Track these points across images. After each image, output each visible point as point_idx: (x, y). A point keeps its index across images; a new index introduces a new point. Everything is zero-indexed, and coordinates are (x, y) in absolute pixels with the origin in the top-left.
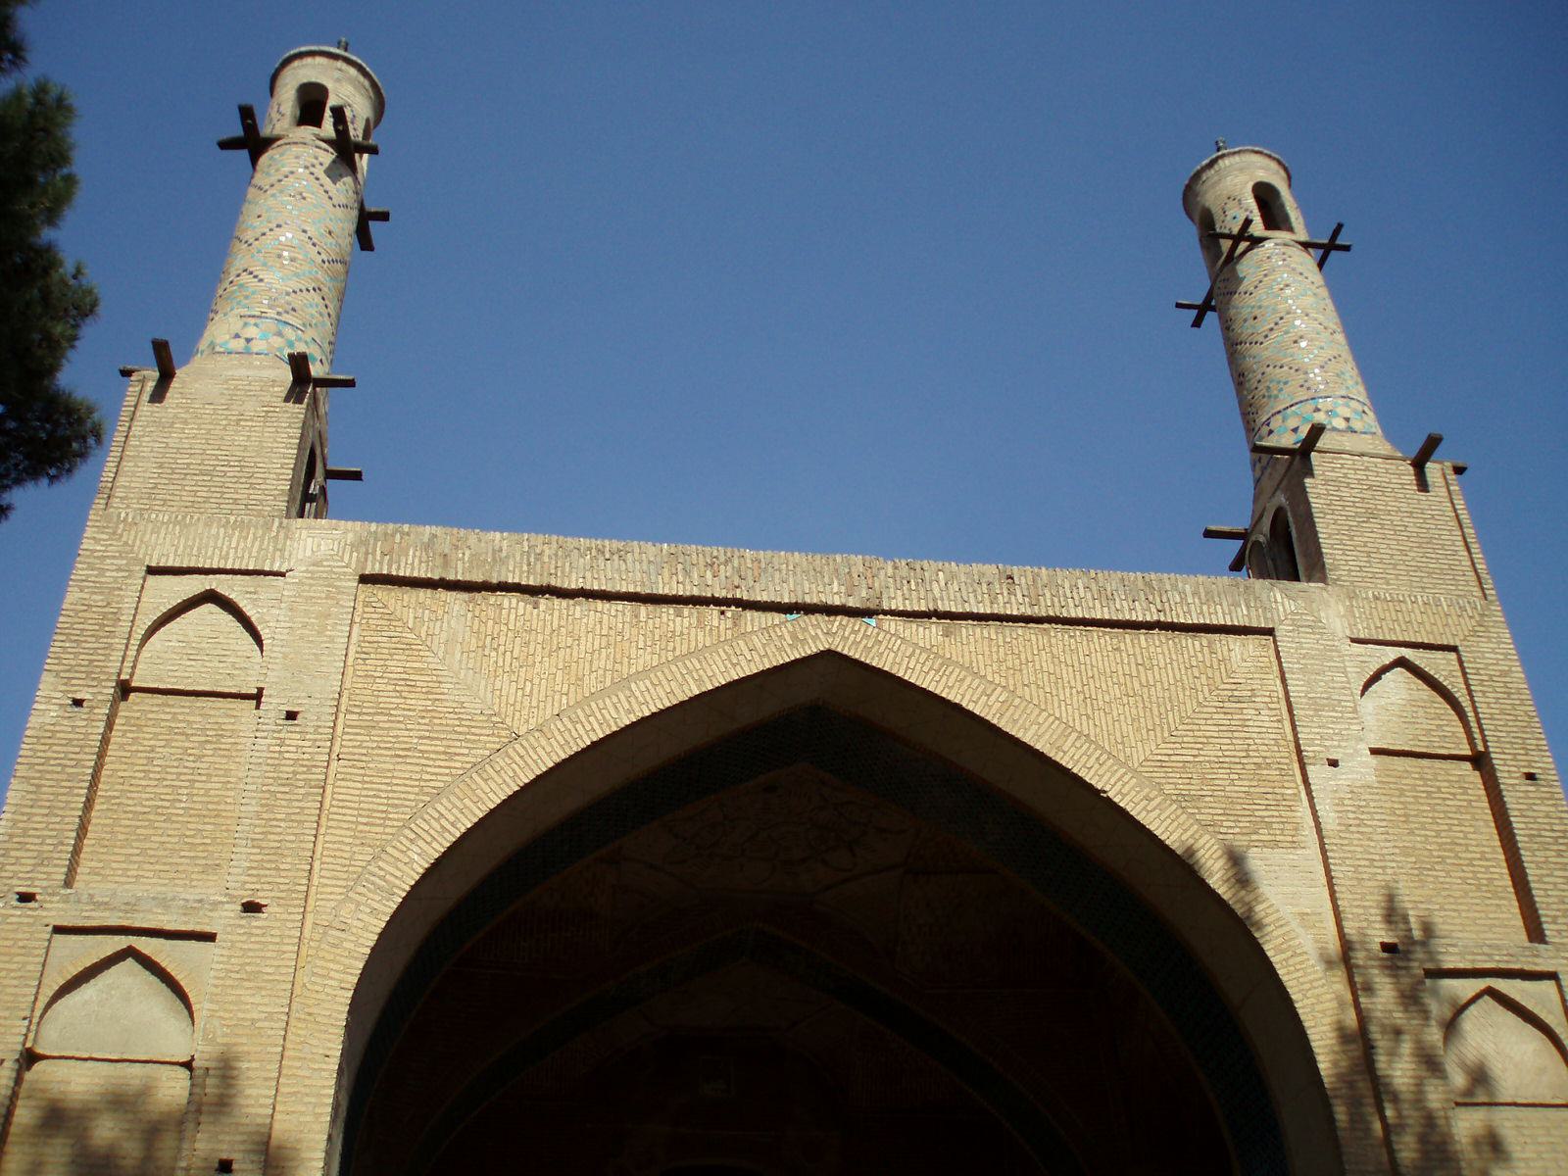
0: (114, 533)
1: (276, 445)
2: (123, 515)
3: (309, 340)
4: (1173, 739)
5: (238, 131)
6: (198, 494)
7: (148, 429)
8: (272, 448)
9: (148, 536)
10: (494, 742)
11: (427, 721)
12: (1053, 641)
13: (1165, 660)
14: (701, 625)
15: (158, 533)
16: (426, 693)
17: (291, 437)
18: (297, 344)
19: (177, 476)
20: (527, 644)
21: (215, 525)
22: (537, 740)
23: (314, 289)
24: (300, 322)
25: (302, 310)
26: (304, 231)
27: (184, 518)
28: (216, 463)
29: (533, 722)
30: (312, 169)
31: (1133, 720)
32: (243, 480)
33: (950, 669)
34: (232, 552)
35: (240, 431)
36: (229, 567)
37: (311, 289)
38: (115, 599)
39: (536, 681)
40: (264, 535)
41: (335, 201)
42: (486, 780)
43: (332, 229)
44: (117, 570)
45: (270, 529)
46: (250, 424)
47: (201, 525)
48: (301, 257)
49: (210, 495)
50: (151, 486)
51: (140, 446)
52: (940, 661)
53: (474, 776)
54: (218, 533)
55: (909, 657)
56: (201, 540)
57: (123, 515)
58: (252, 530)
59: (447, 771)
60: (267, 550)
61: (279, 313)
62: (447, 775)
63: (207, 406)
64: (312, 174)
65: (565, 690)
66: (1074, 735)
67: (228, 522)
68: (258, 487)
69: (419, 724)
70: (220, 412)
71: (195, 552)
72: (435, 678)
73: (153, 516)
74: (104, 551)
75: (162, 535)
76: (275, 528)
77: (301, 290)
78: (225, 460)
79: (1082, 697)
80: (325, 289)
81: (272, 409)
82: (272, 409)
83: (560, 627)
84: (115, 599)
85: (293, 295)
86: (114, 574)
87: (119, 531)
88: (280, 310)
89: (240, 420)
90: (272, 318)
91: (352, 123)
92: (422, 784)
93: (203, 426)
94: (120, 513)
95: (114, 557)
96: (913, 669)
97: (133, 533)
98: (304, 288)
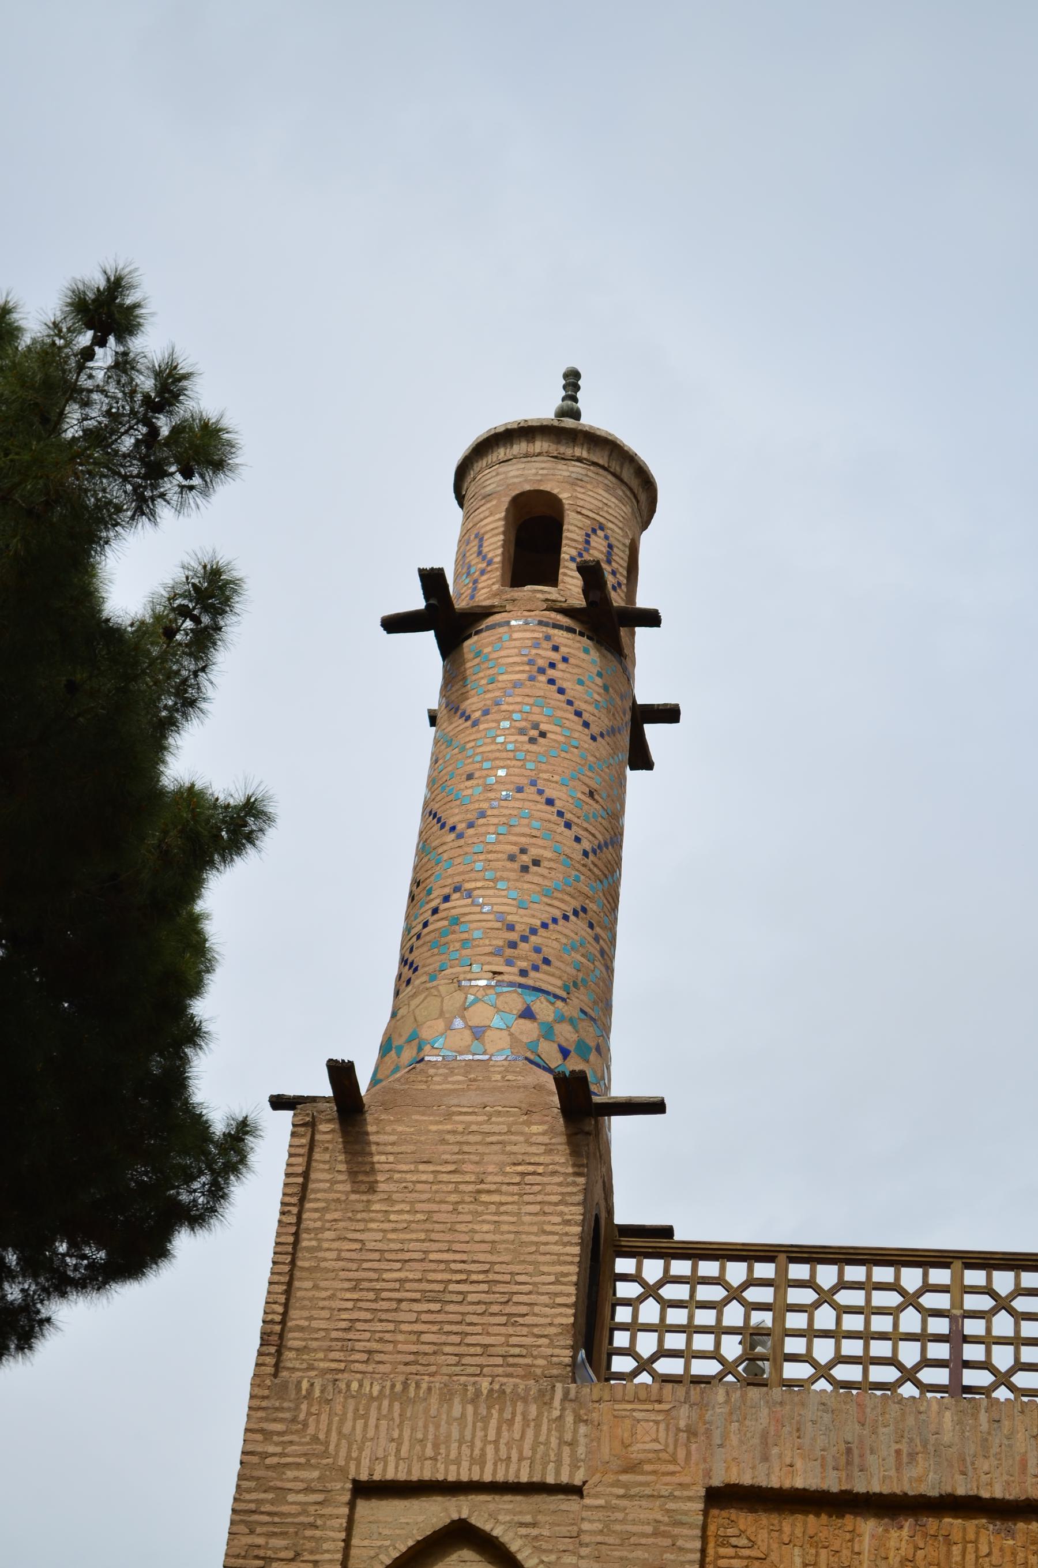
0: (294, 1420)
1: (544, 1238)
2: (305, 1385)
3: (576, 1014)
5: (417, 602)
6: (425, 1338)
7: (328, 1217)
8: (536, 1243)
9: (349, 1424)
15: (366, 1417)
17: (567, 1223)
18: (558, 1028)
19: (385, 1305)
21: (457, 1400)
23: (576, 913)
24: (559, 983)
25: (560, 958)
26: (550, 802)
27: (405, 1385)
28: (447, 1276)
30: (551, 673)
32: (495, 1308)
34: (490, 1450)
35: (482, 1214)
36: (487, 1478)
37: (570, 914)
38: (309, 1545)
40: (539, 1415)
41: (595, 729)
43: (594, 785)
44: (308, 1490)
45: (549, 1404)
46: (496, 1198)
47: (434, 1400)
48: (548, 854)
49: (443, 1338)
50: (344, 1325)
51: (319, 1249)
54: (463, 1415)
56: (437, 1427)
57: (305, 1385)
58: (520, 1407)
60: (547, 1443)
61: (523, 973)
63: (421, 1167)
64: (551, 682)
67: (478, 1393)
68: (520, 1320)
70: (445, 1177)
71: (429, 1452)
73: (355, 1386)
74: (282, 1455)
75: (372, 1421)
76: (557, 1403)
77: (555, 921)
78: (460, 1272)
80: (591, 906)
81: (531, 1168)
82: (531, 1168)
84: (309, 1545)
85: (542, 932)
86: (301, 1498)
87: (302, 1416)
88: (524, 964)
89: (479, 1192)
90: (511, 984)
91: (609, 562)
93: (419, 1206)
94: (299, 1383)
95: (298, 1466)
97: (324, 1417)
98: (558, 914)
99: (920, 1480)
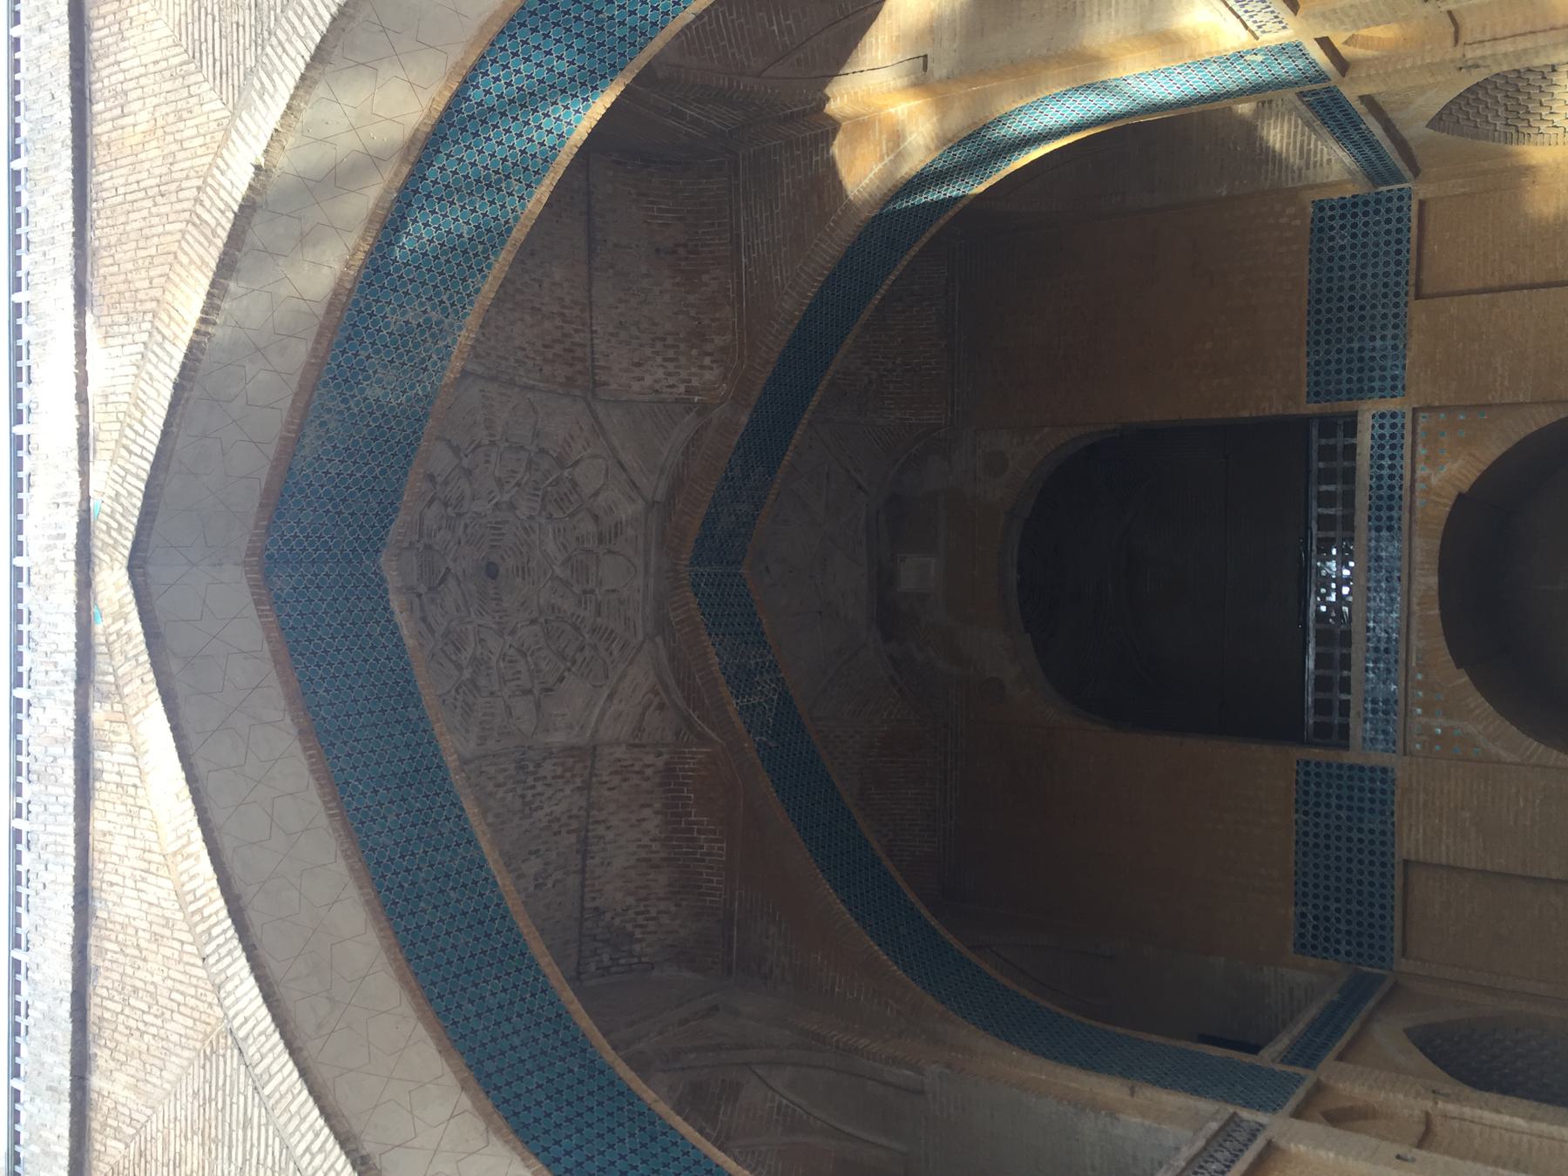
4: (197, 55)
10: (232, 1056)
11: (213, 1147)
12: (104, 242)
13: (116, 73)
14: (108, 747)
16: (186, 1139)
20: (136, 990)
22: (229, 994)
29: (211, 998)
31: (181, 119)
33: (141, 395)
39: (169, 983)
42: (271, 1077)
52: (133, 409)
53: (267, 1091)
55: (130, 452)
59: (263, 1129)
62: (267, 1131)
65: (177, 945)
66: (199, 210)
69: (216, 1158)
72: (172, 1126)
79: (159, 200)
83: (117, 942)
92: (277, 1168)
96: (143, 448)
99: (64, 1036)
